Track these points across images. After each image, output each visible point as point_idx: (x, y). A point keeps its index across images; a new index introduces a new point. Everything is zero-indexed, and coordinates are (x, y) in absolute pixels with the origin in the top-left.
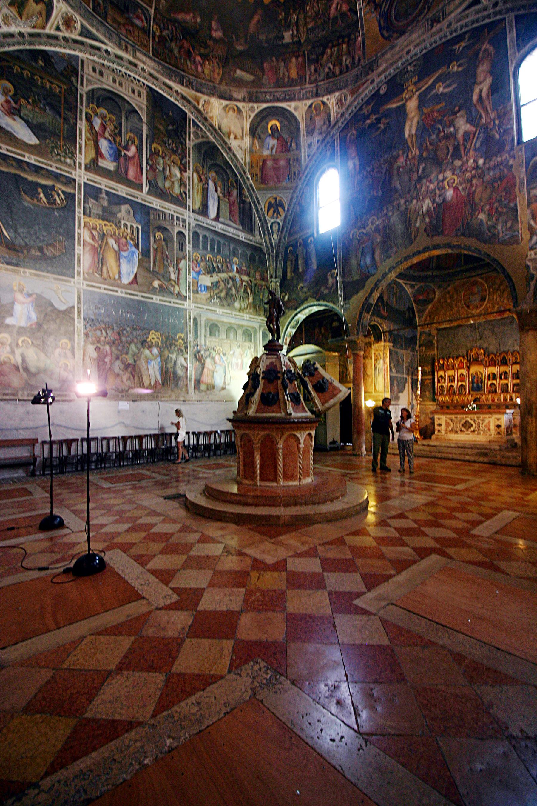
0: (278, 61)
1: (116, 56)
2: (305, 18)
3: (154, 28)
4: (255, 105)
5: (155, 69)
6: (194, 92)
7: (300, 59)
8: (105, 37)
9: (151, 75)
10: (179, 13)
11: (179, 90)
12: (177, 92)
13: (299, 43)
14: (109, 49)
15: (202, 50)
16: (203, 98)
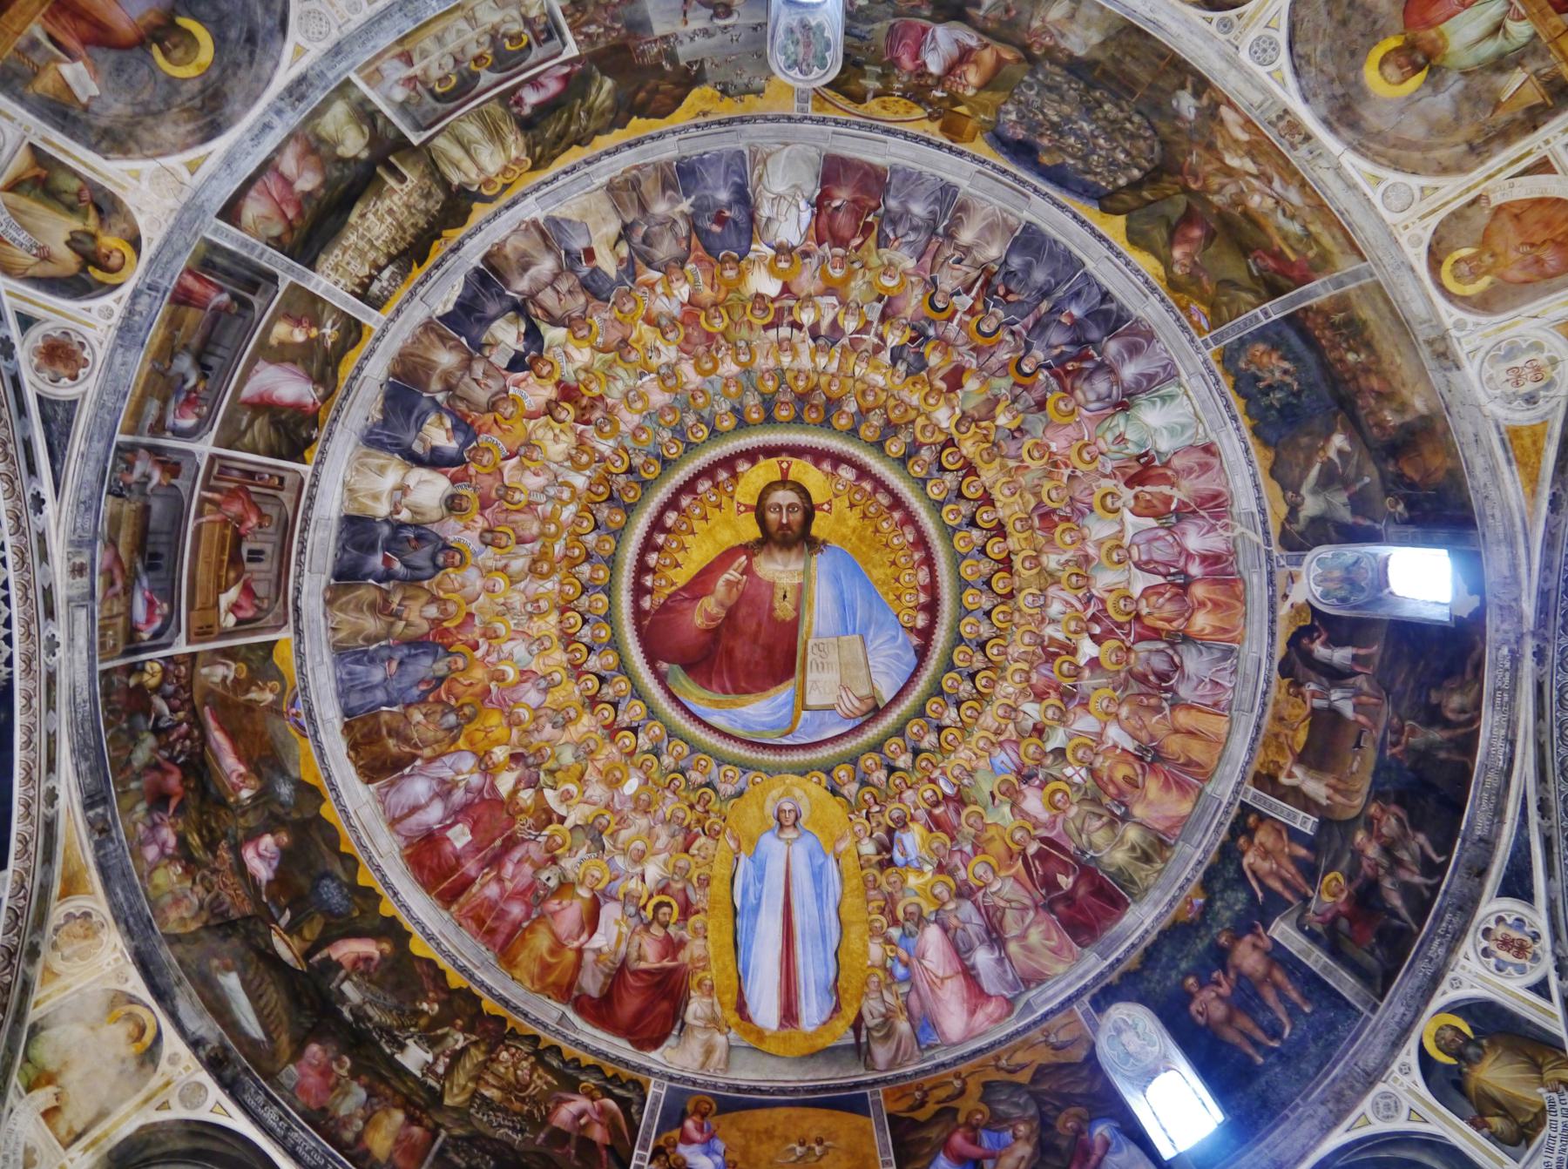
0: (354, 1074)
1: (42, 537)
2: (484, 1066)
3: (152, 662)
4: (215, 1093)
5: (73, 688)
6: (90, 858)
7: (417, 1131)
8: (79, 488)
9: (51, 679)
10: (222, 728)
11: (62, 803)
12: (52, 797)
13: (436, 1097)
14: (50, 508)
15: (194, 840)
16: (95, 901)
